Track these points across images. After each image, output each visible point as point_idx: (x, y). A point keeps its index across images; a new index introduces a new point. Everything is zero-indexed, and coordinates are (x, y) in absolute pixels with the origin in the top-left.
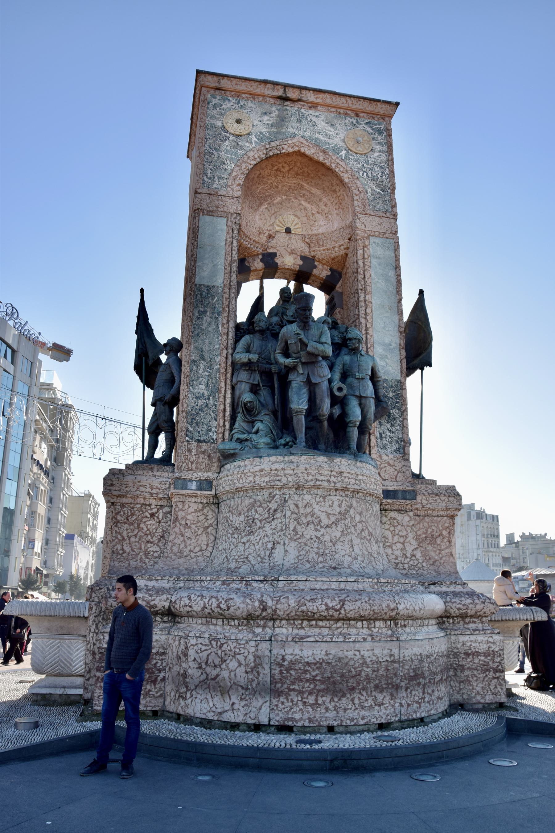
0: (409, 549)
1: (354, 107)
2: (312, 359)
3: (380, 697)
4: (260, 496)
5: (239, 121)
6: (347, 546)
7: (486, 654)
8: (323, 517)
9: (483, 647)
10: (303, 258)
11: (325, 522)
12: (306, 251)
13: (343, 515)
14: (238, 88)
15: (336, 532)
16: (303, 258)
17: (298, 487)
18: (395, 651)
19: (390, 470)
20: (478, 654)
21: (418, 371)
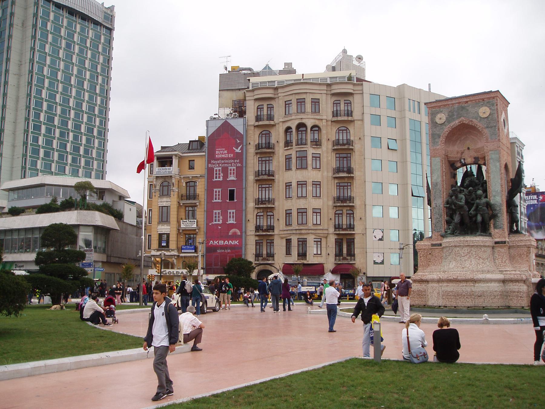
0: (504, 260)
1: (481, 98)
2: (461, 207)
3: (468, 300)
4: (448, 249)
5: (440, 119)
6: (469, 262)
7: (518, 292)
8: (462, 254)
9: (517, 290)
10: (475, 158)
11: (463, 255)
12: (476, 155)
13: (469, 253)
14: (439, 105)
15: (466, 258)
16: (475, 158)
17: (455, 246)
18: (473, 289)
19: (497, 235)
20: (515, 292)
21: (519, 194)
